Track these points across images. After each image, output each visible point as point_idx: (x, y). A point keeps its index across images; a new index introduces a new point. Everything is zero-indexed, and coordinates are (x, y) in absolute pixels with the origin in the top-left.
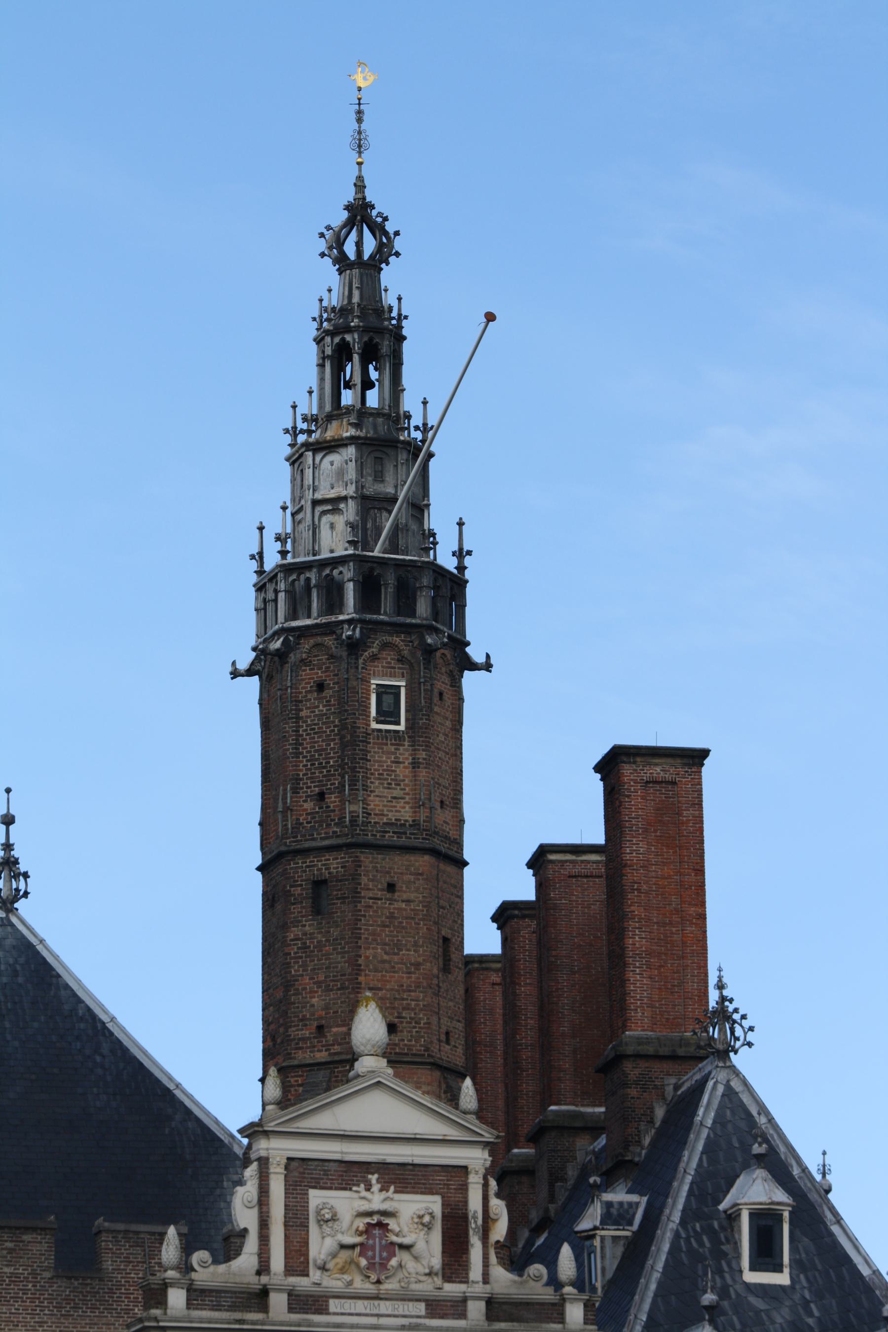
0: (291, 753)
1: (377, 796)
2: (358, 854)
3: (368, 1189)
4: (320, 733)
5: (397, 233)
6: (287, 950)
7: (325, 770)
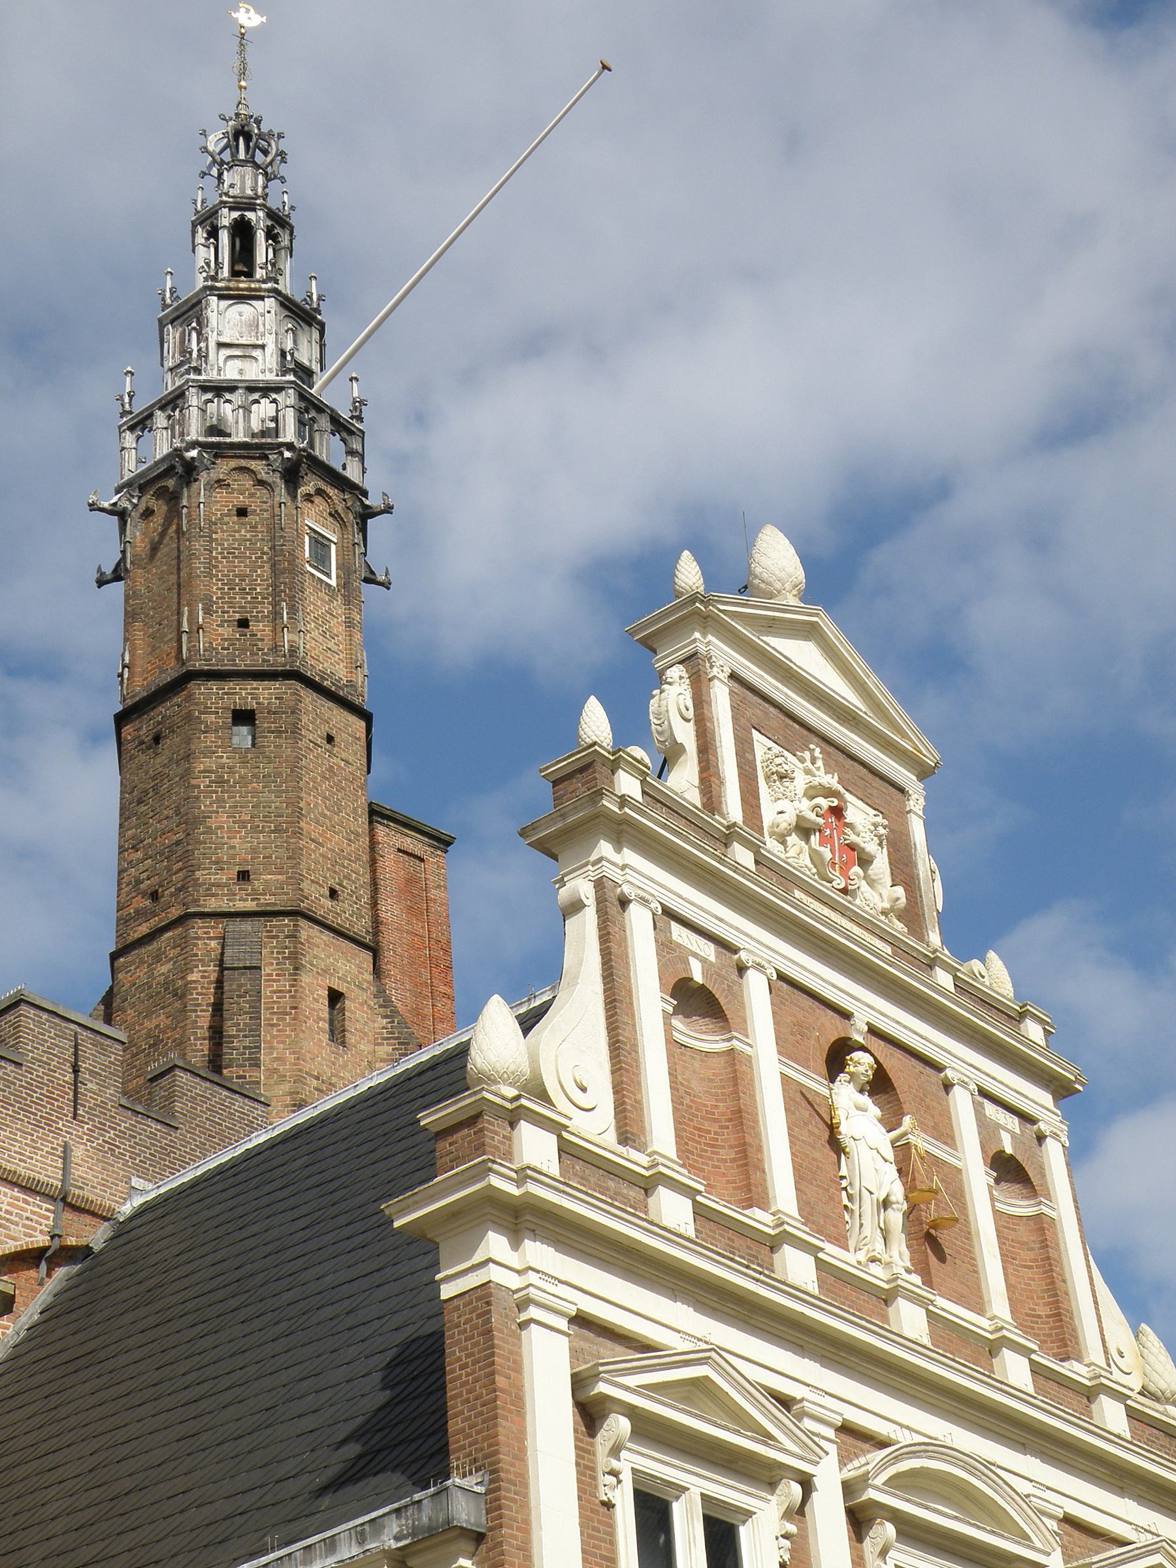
4: (242, 557)
6: (193, 782)
7: (249, 597)
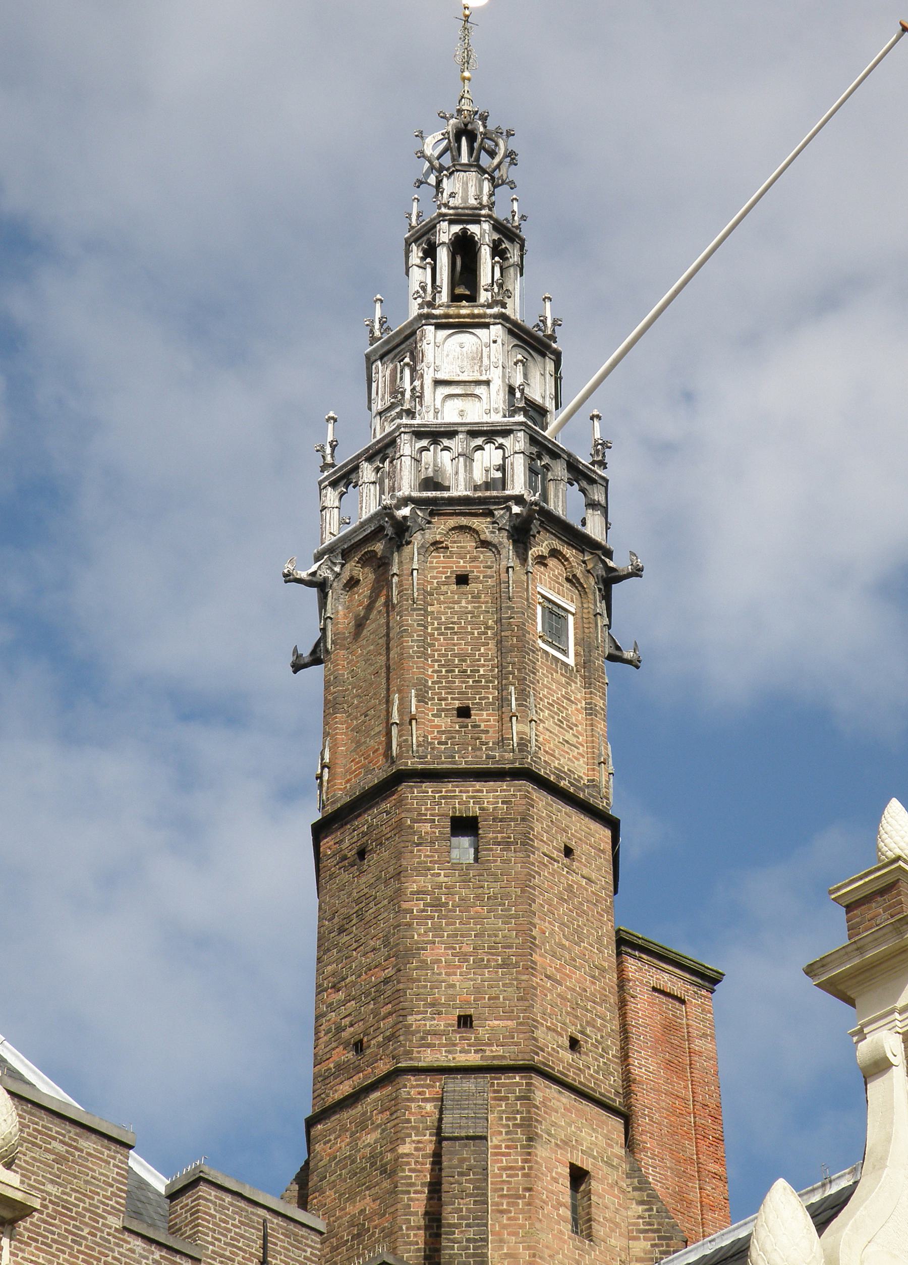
2: (530, 790)
4: (462, 633)
6: (405, 906)
7: (471, 681)
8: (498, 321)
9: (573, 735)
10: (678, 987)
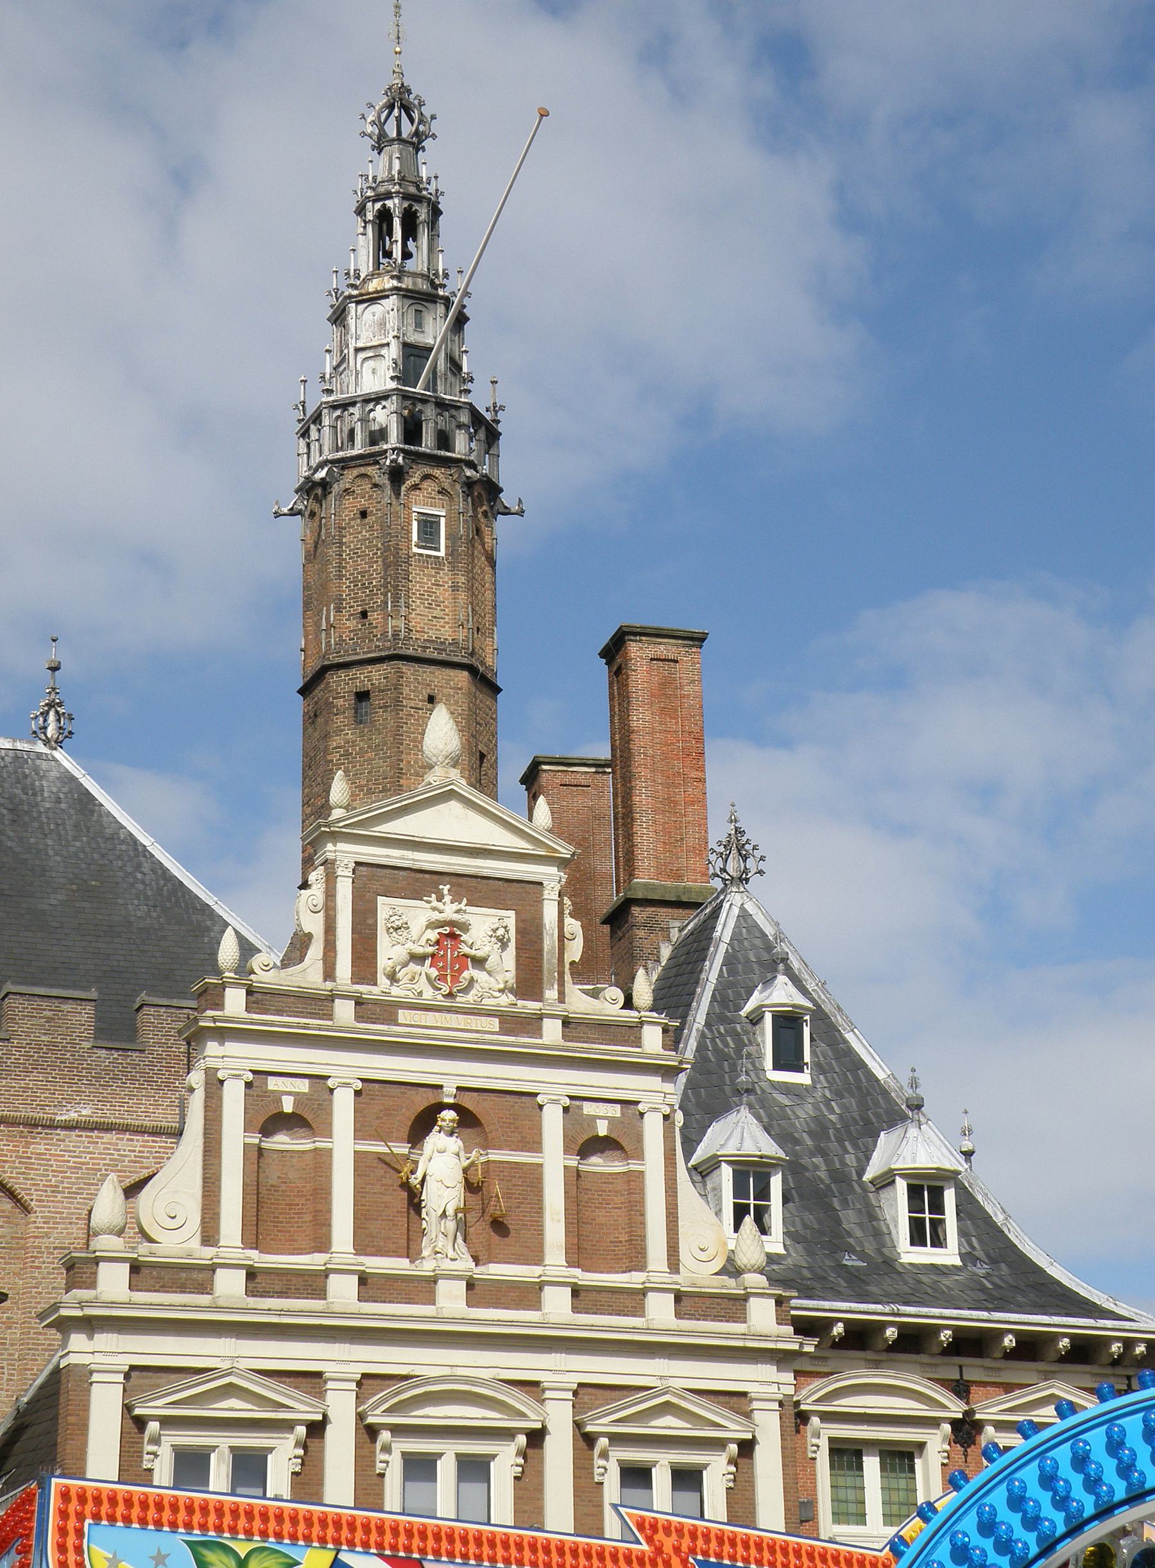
0: (334, 576)
1: (419, 614)
3: (439, 900)
5: (433, 117)
6: (329, 758)
8: (394, 292)
9: (441, 610)
10: (673, 653)
